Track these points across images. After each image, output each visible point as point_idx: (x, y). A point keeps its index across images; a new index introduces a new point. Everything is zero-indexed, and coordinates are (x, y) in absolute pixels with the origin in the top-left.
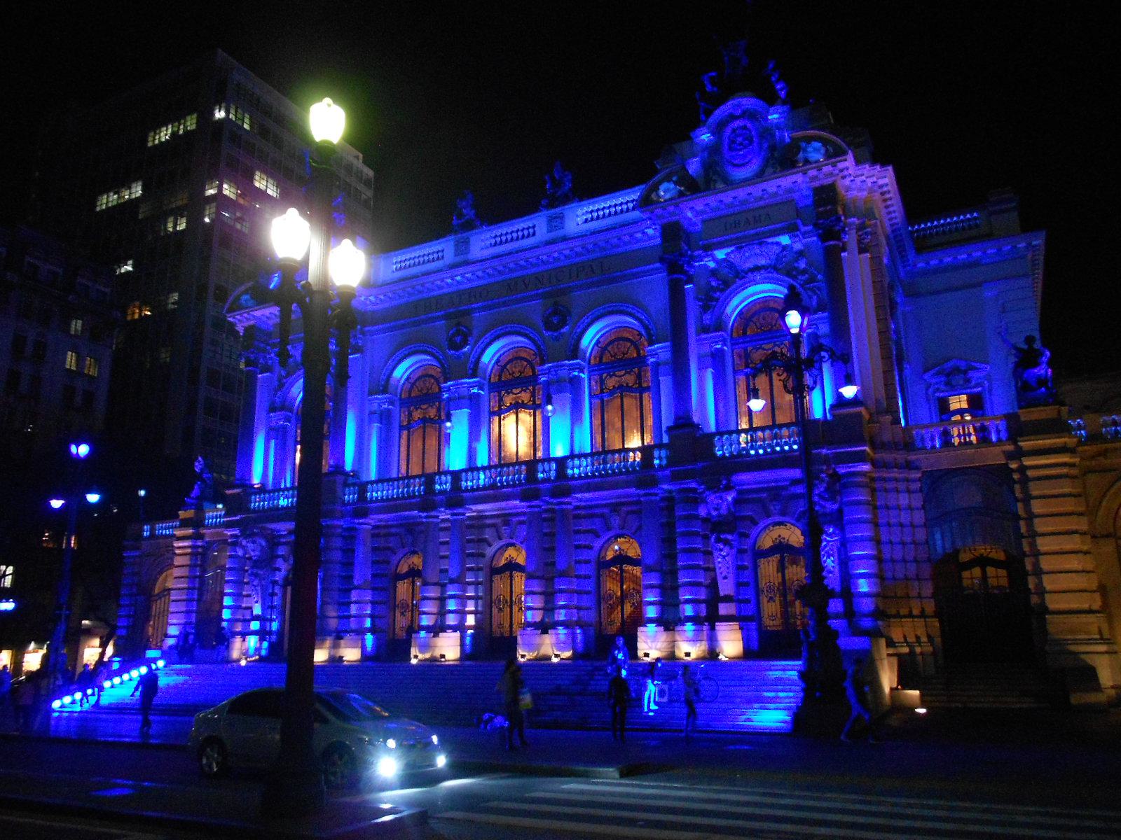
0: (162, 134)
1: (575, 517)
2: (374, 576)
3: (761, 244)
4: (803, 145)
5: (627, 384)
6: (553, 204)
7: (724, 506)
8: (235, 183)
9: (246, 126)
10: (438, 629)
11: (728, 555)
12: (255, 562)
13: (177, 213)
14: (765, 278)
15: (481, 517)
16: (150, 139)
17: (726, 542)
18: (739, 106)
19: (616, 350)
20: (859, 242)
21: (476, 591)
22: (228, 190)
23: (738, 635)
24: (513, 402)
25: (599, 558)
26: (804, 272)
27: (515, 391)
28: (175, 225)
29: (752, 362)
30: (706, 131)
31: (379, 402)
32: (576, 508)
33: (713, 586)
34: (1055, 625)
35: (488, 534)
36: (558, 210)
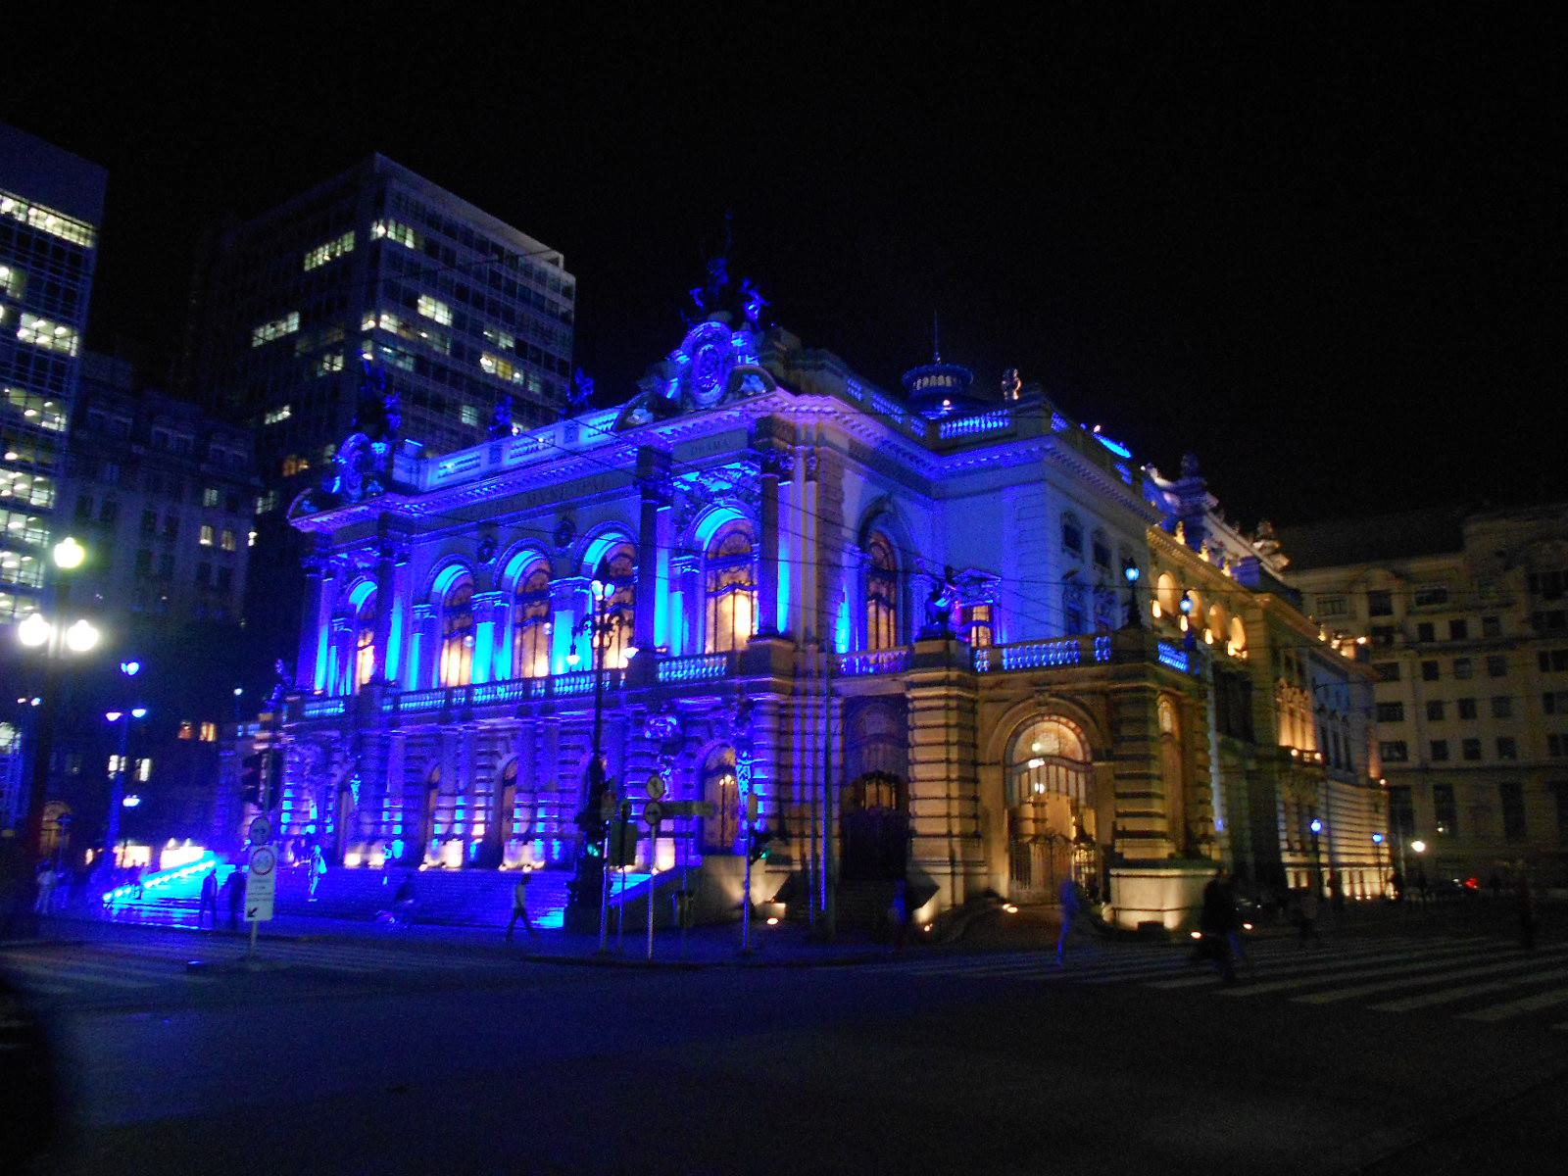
0: (320, 256)
1: (562, 733)
2: (406, 784)
4: (746, 377)
8: (392, 311)
9: (409, 244)
10: (446, 838)
13: (334, 351)
15: (493, 730)
16: (307, 261)
18: (710, 327)
20: (808, 469)
21: (487, 802)
22: (388, 323)
28: (332, 364)
31: (421, 611)
32: (564, 724)
34: (919, 846)
35: (500, 747)
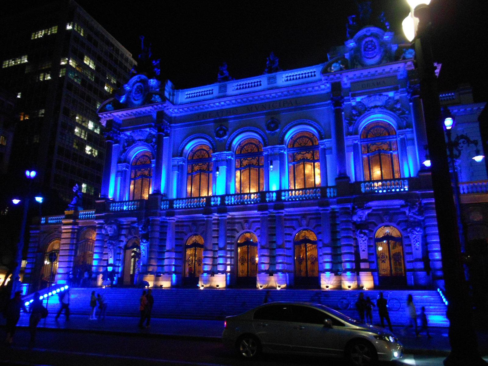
0: (39, 34)
1: (285, 220)
3: (380, 95)
4: (404, 50)
5: (307, 158)
6: (270, 72)
7: (364, 217)
8: (75, 59)
9: (82, 34)
10: (213, 273)
11: (365, 240)
12: (111, 237)
13: (46, 72)
14: (379, 111)
15: (233, 218)
16: (33, 36)
17: (365, 234)
18: (369, 30)
19: (301, 142)
21: (231, 254)
22: (72, 63)
23: (371, 278)
24: (248, 164)
25: (294, 240)
26: (399, 109)
27: (248, 159)
28: (44, 78)
29: (370, 150)
30: (353, 41)
31: (178, 161)
32: (285, 215)
33: (357, 254)
35: (236, 227)
36: (273, 74)
